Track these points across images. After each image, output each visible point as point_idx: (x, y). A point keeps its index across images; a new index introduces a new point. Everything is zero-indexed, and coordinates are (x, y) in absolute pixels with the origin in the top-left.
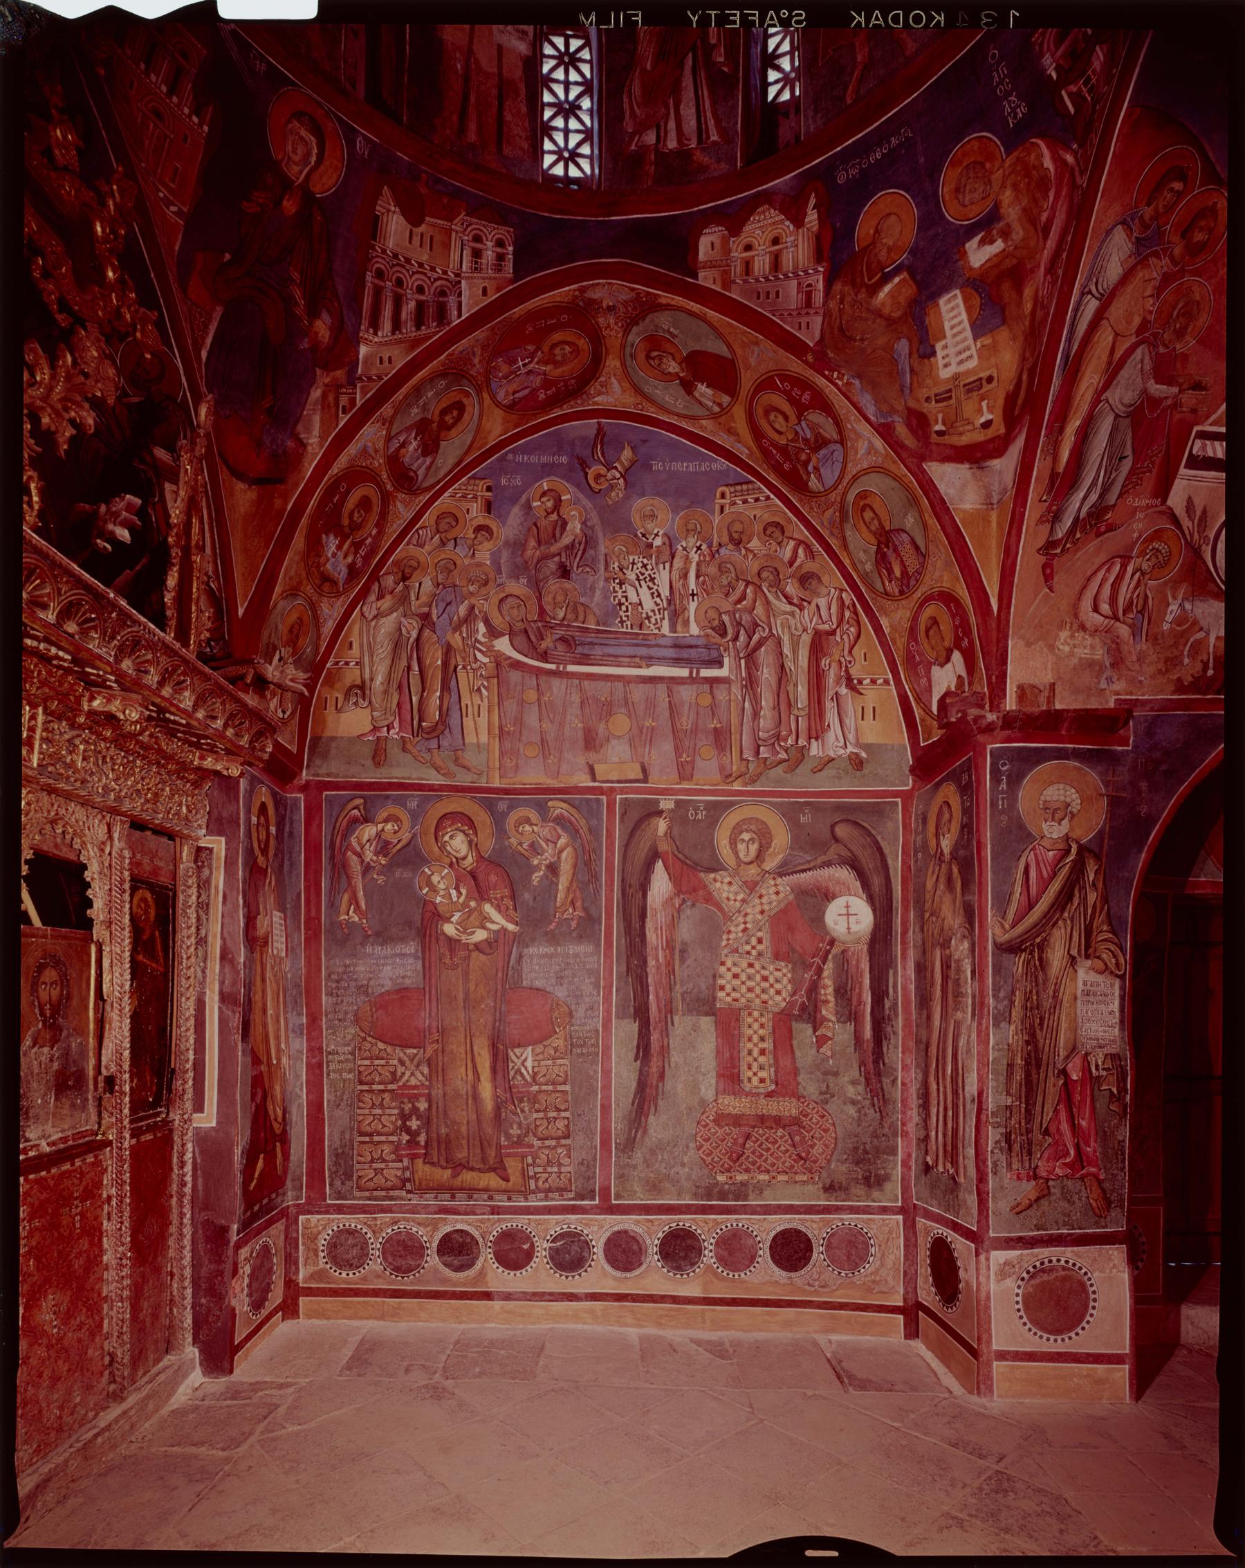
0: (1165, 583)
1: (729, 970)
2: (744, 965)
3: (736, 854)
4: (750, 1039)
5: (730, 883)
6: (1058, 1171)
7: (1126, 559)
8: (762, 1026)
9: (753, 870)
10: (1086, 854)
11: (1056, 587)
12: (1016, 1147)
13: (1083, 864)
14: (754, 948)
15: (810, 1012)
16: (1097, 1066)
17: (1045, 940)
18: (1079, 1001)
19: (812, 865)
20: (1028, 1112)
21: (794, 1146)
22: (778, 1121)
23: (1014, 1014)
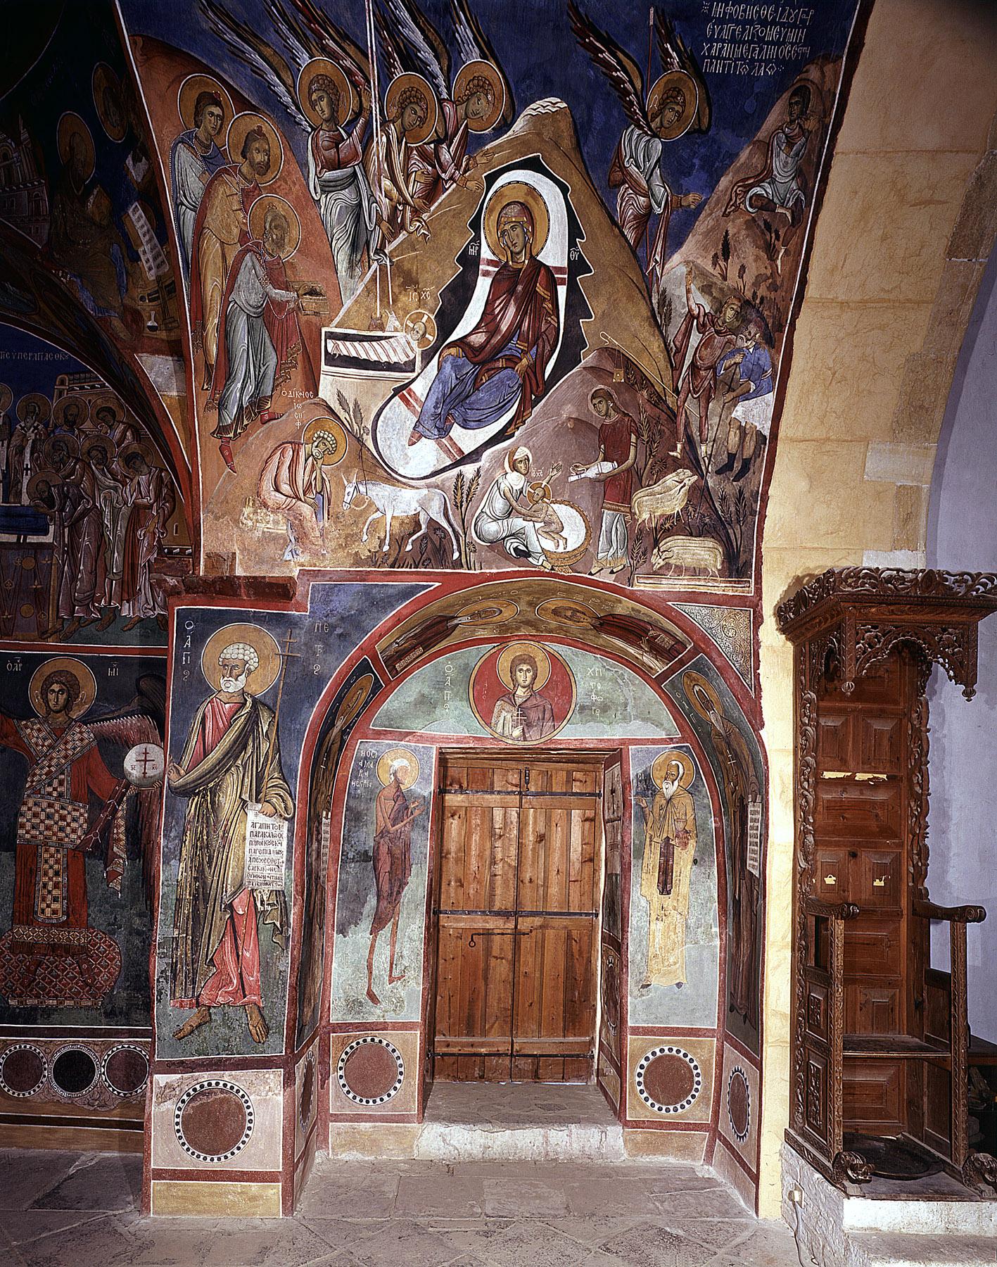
0: (338, 468)
1: (29, 809)
2: (45, 805)
3: (47, 702)
4: (46, 874)
5: (39, 730)
6: (220, 999)
7: (296, 446)
8: (57, 862)
9: (61, 718)
10: (260, 707)
11: (237, 468)
12: (181, 977)
13: (258, 716)
14: (55, 789)
15: (102, 851)
16: (262, 901)
17: (217, 785)
18: (247, 842)
19: (116, 714)
20: (195, 943)
21: (81, 973)
22: (67, 950)
23: (184, 853)
